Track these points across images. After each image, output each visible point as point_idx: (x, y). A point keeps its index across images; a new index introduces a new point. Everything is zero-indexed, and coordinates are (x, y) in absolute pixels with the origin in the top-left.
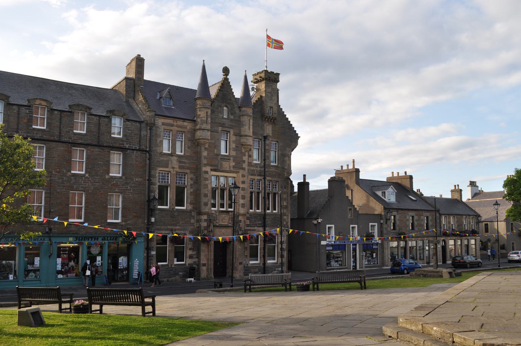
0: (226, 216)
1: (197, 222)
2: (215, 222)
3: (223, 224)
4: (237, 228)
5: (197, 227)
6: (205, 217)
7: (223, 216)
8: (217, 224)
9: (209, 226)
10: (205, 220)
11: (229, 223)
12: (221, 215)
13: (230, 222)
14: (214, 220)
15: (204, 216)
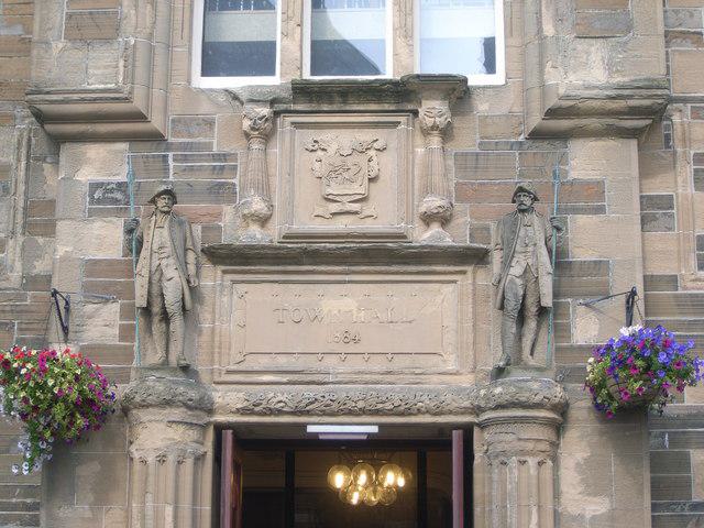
0: (381, 136)
1: (28, 228)
2: (228, 210)
3: (341, 225)
4: (516, 270)
5: (31, 281)
6: (99, 164)
7: (338, 141)
8: (255, 235)
9: (135, 243)
10: (106, 198)
11: (428, 219)
12: (311, 135)
13: (433, 203)
14: (222, 192)
15: (94, 151)
